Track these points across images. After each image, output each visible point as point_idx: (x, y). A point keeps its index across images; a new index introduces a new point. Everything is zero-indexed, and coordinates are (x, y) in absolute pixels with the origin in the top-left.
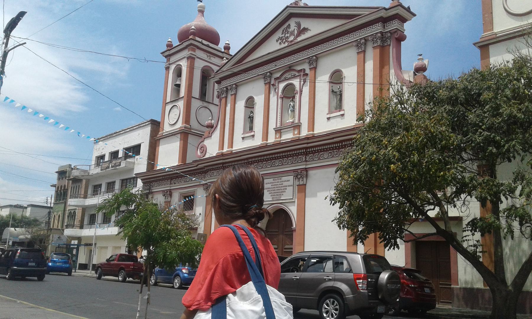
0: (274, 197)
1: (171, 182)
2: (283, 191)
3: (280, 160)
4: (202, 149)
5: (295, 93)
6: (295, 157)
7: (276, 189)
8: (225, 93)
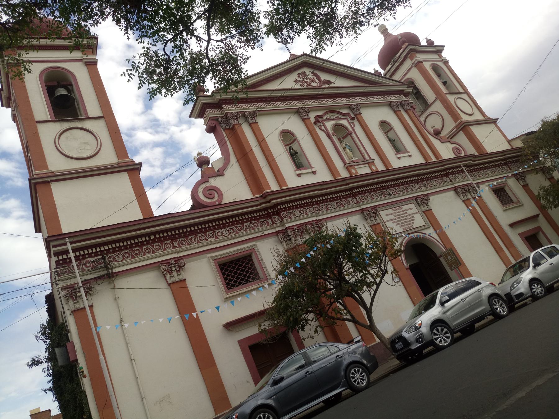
0: (405, 227)
1: (173, 244)
2: (411, 219)
3: (391, 189)
5: (350, 134)
6: (406, 186)
7: (402, 219)
8: (239, 119)
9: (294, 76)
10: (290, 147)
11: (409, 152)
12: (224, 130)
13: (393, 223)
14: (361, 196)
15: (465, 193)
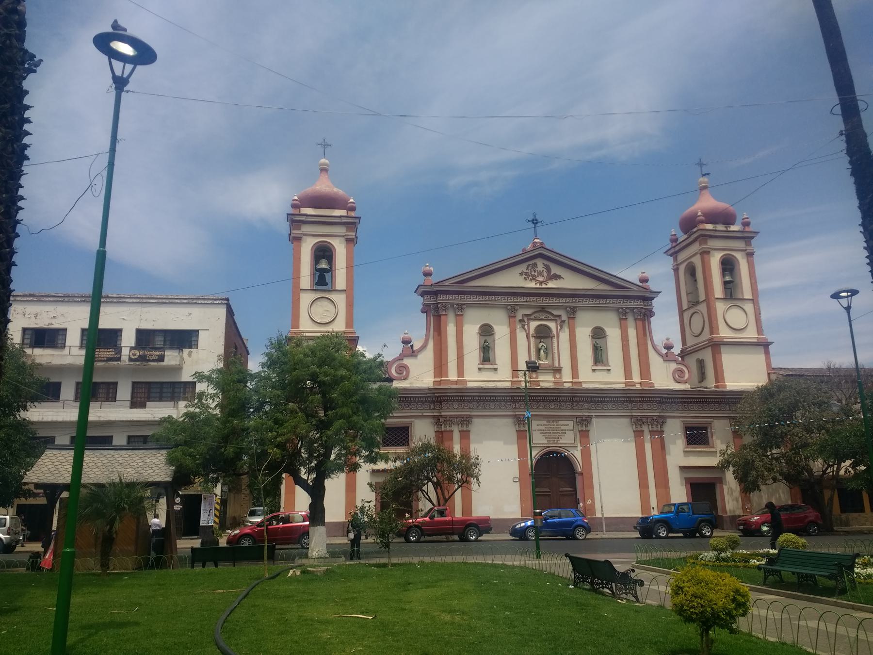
4: (402, 368)
5: (552, 337)
9: (523, 268)
10: (485, 340)
11: (610, 366)
12: (433, 315)
13: (541, 433)
14: (521, 403)
15: (640, 425)
